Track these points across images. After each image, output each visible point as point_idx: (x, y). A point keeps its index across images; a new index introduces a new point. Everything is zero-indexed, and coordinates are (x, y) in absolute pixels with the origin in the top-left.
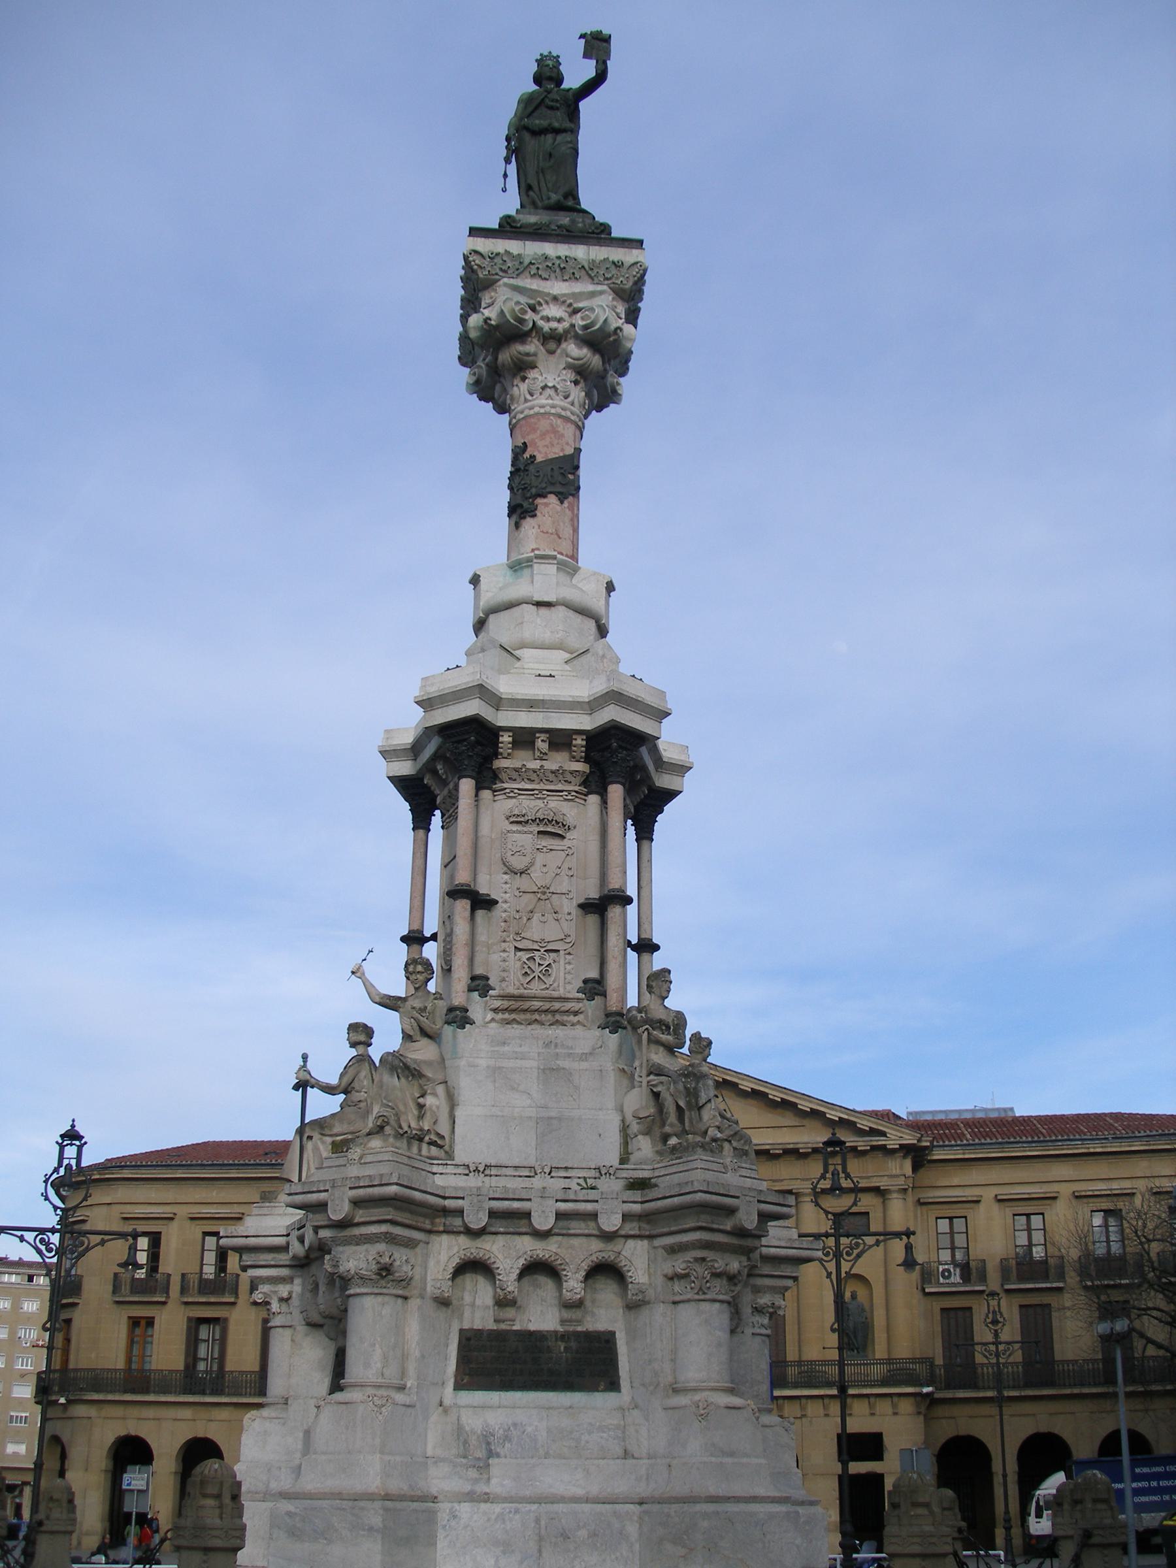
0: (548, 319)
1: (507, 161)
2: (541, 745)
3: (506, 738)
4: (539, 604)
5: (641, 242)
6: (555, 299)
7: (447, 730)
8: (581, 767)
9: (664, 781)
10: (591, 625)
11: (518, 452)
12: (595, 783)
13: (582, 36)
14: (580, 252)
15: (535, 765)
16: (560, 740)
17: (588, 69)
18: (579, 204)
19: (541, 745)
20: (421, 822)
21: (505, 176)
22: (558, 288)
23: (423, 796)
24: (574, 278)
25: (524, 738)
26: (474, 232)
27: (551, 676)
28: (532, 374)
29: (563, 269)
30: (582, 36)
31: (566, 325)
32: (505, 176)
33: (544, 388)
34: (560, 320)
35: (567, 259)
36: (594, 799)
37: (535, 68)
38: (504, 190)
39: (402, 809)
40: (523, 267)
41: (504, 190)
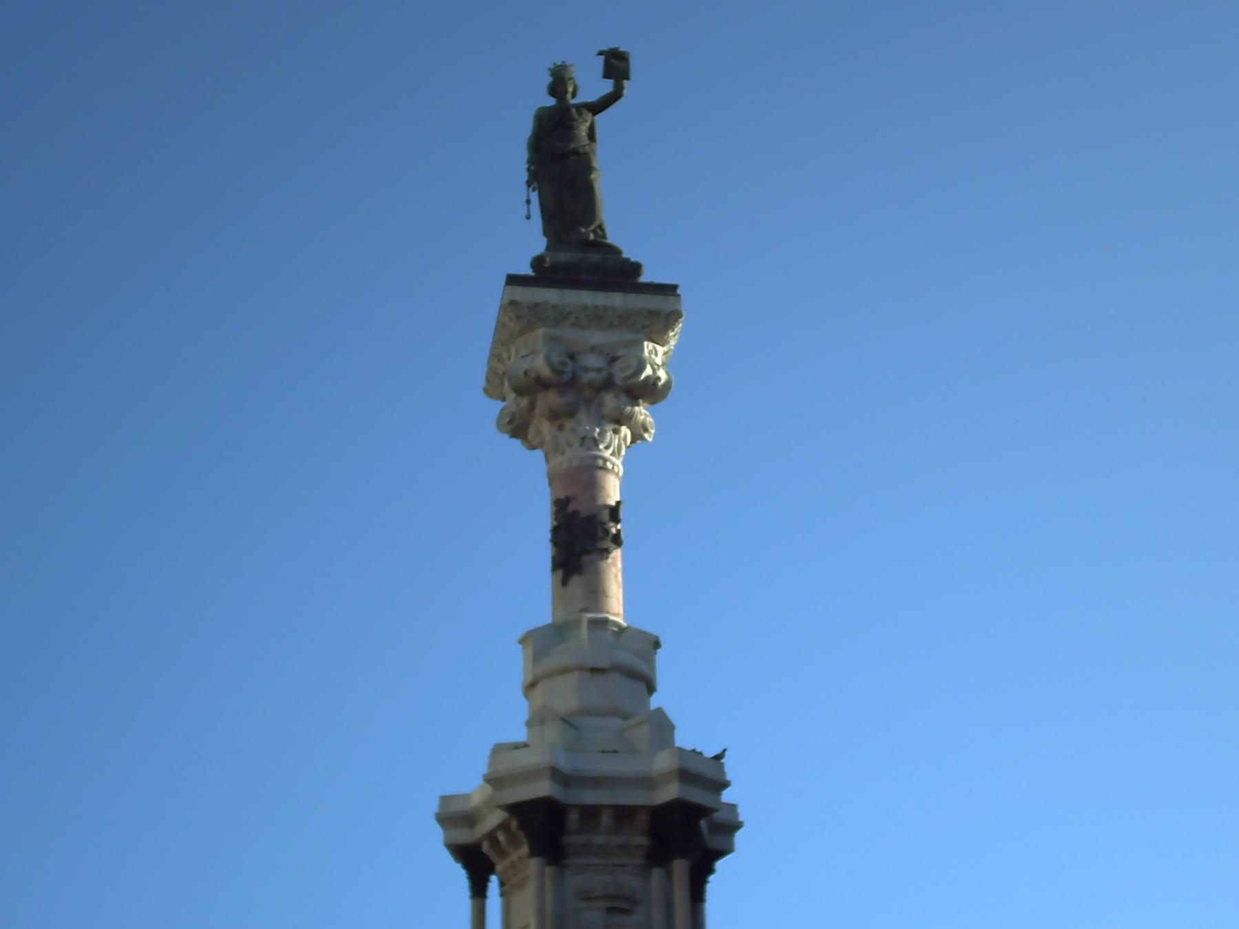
0: (586, 369)
1: (529, 184)
2: (606, 819)
3: (573, 817)
4: (595, 671)
5: (675, 287)
6: (593, 349)
7: (516, 809)
8: (643, 840)
9: (714, 842)
10: (641, 687)
11: (561, 506)
12: (658, 856)
13: (600, 53)
14: (616, 300)
15: (599, 840)
16: (623, 814)
17: (608, 86)
18: (604, 237)
19: (606, 819)
20: (479, 891)
21: (528, 202)
22: (598, 337)
23: (476, 862)
24: (611, 326)
25: (591, 813)
26: (513, 280)
27: (615, 752)
28: (569, 424)
29: (597, 318)
30: (600, 53)
31: (604, 375)
32: (528, 202)
33: (584, 438)
34: (599, 370)
35: (605, 308)
36: (657, 873)
37: (549, 80)
38: (528, 218)
39: (459, 876)
40: (561, 316)
41: (528, 218)
